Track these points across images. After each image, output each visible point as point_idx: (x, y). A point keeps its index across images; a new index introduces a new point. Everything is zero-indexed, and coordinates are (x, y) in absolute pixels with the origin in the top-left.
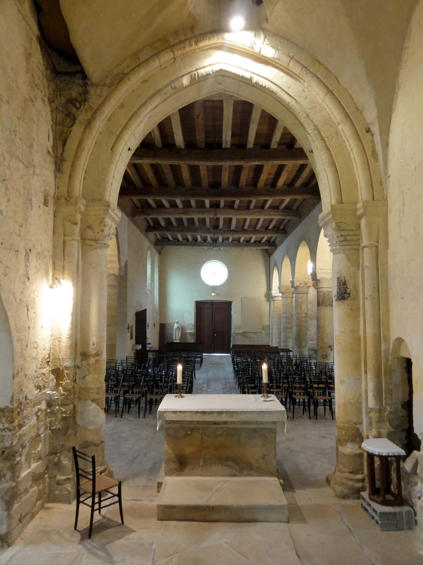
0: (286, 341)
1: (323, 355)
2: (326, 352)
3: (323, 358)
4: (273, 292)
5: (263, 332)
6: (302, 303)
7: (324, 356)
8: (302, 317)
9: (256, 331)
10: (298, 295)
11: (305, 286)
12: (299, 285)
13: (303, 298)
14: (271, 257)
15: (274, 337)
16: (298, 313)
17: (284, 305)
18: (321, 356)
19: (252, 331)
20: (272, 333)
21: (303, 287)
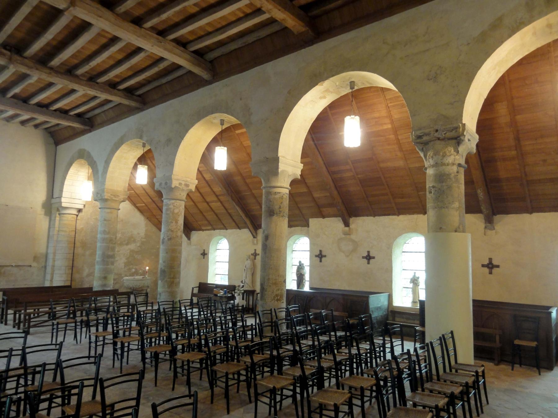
0: (105, 278)
1: (277, 295)
2: (281, 290)
3: (278, 300)
4: (63, 200)
5: (34, 264)
6: (179, 215)
7: (279, 298)
8: (178, 236)
9: (20, 264)
10: (173, 201)
11: (185, 188)
12: (178, 185)
13: (181, 207)
14: (57, 147)
15: (56, 272)
16: (172, 231)
17: (105, 220)
18: (274, 297)
19: (14, 264)
20: (53, 266)
21: (183, 190)
